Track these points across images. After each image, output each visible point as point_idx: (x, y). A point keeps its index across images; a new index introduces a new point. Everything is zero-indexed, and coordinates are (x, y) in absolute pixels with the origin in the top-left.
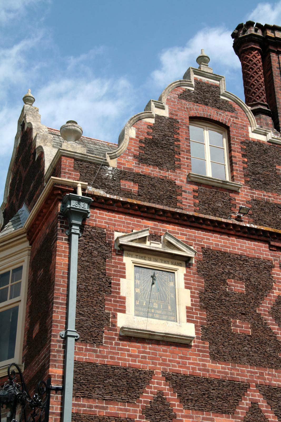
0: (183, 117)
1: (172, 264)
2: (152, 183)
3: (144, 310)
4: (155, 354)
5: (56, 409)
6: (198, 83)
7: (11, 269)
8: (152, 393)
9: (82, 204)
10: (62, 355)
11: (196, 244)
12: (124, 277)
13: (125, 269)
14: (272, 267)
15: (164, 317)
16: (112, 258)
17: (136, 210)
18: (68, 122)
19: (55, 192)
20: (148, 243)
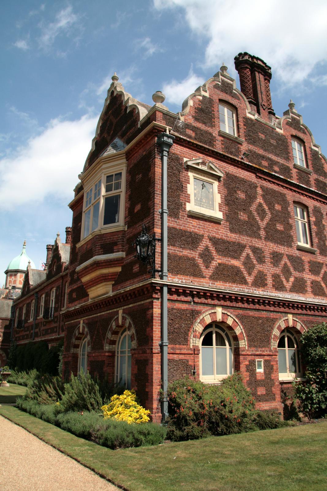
0: (216, 99)
1: (212, 179)
2: (201, 133)
3: (199, 203)
4: (205, 226)
5: (159, 250)
6: (223, 81)
7: (114, 174)
8: (203, 246)
9: (169, 139)
10: (160, 222)
11: (223, 170)
12: (189, 183)
13: (189, 179)
14: (257, 187)
15: (208, 207)
16: (183, 172)
17: (194, 147)
18: (157, 92)
19: (154, 131)
20: (200, 166)
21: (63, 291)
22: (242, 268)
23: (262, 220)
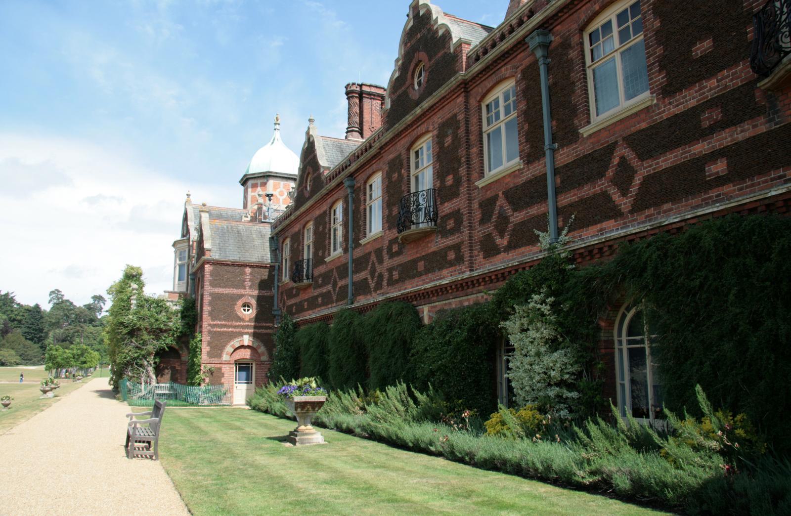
21: (474, 128)
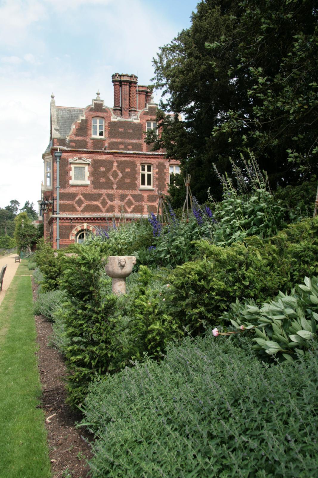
3: (76, 179)
22: (100, 205)
23: (115, 179)
